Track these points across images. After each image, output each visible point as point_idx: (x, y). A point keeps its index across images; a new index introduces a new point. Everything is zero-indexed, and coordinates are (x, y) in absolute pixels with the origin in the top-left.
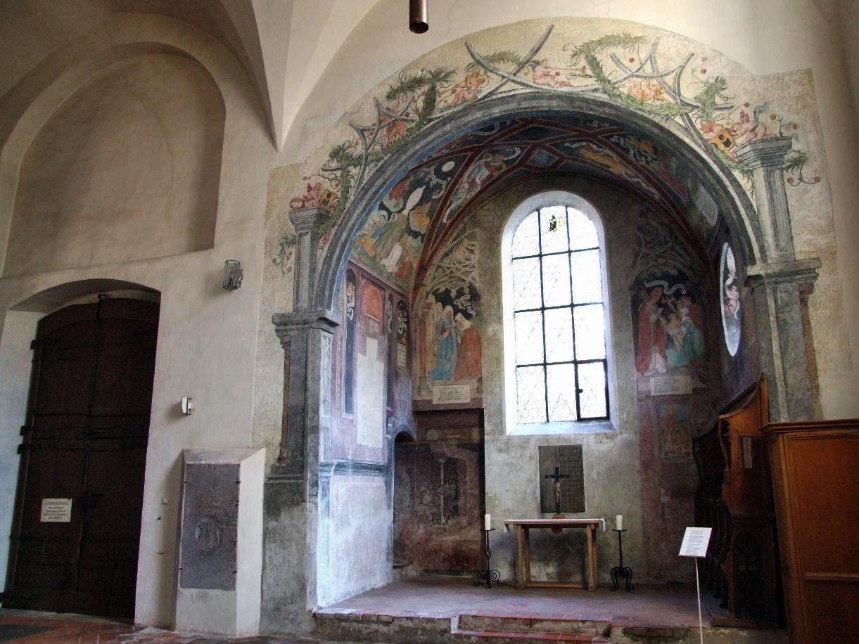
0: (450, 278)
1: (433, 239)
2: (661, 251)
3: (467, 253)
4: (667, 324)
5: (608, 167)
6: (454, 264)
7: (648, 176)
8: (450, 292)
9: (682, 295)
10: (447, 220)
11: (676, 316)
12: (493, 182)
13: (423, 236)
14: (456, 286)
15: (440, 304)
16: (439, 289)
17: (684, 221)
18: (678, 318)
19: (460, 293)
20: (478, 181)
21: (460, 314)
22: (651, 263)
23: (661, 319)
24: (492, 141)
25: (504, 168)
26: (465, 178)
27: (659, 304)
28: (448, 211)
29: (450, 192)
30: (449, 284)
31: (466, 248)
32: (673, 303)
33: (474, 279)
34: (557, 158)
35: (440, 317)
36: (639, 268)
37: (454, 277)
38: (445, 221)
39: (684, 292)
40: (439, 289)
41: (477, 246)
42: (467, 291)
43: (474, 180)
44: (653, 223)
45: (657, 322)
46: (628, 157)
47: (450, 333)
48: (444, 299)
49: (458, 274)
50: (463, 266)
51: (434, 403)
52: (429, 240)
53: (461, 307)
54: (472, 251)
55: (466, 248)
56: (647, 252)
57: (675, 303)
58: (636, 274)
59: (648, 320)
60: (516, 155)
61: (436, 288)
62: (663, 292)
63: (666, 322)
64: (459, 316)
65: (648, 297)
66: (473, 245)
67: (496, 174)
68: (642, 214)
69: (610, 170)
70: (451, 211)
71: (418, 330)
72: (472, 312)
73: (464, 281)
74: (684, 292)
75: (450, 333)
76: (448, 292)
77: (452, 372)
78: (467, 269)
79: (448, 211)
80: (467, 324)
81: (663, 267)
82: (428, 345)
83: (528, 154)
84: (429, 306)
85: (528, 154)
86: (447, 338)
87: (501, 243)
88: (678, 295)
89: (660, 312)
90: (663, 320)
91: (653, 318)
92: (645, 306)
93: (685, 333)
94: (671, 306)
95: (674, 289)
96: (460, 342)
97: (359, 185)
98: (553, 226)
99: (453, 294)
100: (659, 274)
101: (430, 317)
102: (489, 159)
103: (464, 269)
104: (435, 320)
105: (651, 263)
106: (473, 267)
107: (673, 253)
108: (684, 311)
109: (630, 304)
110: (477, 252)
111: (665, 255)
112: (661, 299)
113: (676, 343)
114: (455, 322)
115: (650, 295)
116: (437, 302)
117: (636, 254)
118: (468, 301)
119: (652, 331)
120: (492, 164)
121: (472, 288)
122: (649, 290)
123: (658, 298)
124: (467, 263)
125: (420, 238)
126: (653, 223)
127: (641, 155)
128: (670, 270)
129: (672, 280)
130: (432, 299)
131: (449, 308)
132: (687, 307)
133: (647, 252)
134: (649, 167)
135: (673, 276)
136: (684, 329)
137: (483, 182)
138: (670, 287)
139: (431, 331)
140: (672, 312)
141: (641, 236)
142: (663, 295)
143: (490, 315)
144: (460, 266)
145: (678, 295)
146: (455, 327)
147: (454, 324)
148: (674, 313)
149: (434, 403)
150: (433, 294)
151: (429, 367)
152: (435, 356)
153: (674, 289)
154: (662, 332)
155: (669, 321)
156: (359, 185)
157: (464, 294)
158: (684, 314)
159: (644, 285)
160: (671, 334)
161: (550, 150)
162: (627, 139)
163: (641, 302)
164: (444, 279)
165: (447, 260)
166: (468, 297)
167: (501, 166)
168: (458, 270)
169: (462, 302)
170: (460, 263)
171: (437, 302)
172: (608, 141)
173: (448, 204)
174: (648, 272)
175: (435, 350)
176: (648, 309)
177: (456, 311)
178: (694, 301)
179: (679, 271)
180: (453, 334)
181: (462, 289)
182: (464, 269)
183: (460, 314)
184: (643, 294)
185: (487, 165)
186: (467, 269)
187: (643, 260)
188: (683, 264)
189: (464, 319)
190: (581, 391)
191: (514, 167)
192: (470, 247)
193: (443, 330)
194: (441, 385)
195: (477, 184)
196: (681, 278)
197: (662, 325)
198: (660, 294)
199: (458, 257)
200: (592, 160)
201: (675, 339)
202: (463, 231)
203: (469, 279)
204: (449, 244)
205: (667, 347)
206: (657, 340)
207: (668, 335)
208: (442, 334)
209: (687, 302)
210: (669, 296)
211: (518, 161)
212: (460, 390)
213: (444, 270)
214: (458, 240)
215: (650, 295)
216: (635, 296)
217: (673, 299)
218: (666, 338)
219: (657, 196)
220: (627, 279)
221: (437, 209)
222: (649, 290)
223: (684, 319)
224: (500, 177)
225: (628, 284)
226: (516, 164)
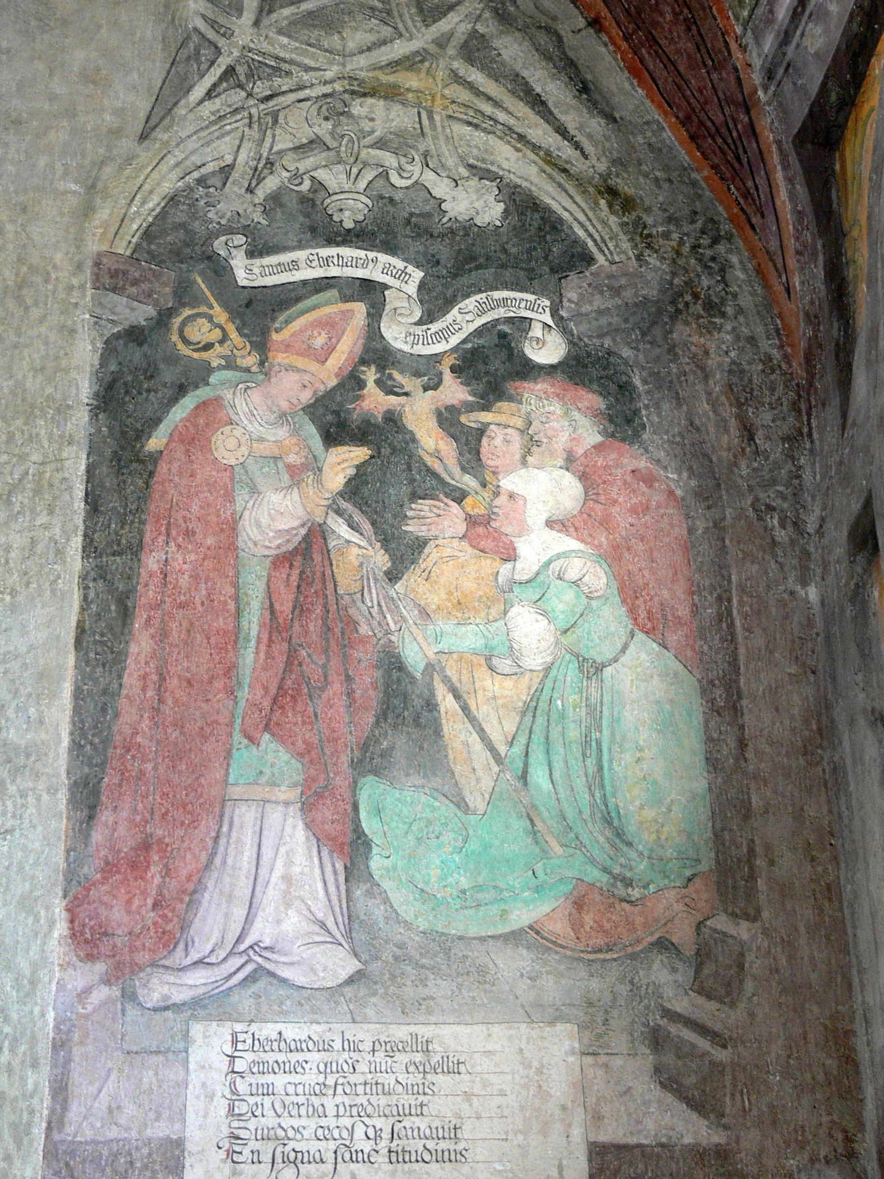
2: (386, 54)
4: (393, 576)
11: (472, 521)
23: (342, 529)
57: (470, 420)
58: (168, 187)
59: (232, 527)
62: (373, 333)
63: (381, 560)
65: (251, 360)
81: (389, 160)
93: (534, 661)
107: (476, 76)
115: (261, 346)
128: (441, 188)
132: (570, 462)
148: (460, 496)
163: (181, 390)
174: (271, 184)
187: (237, 97)
188: (549, 159)
197: (346, 581)
201: (447, 703)
215: (261, 346)
220: (87, 210)
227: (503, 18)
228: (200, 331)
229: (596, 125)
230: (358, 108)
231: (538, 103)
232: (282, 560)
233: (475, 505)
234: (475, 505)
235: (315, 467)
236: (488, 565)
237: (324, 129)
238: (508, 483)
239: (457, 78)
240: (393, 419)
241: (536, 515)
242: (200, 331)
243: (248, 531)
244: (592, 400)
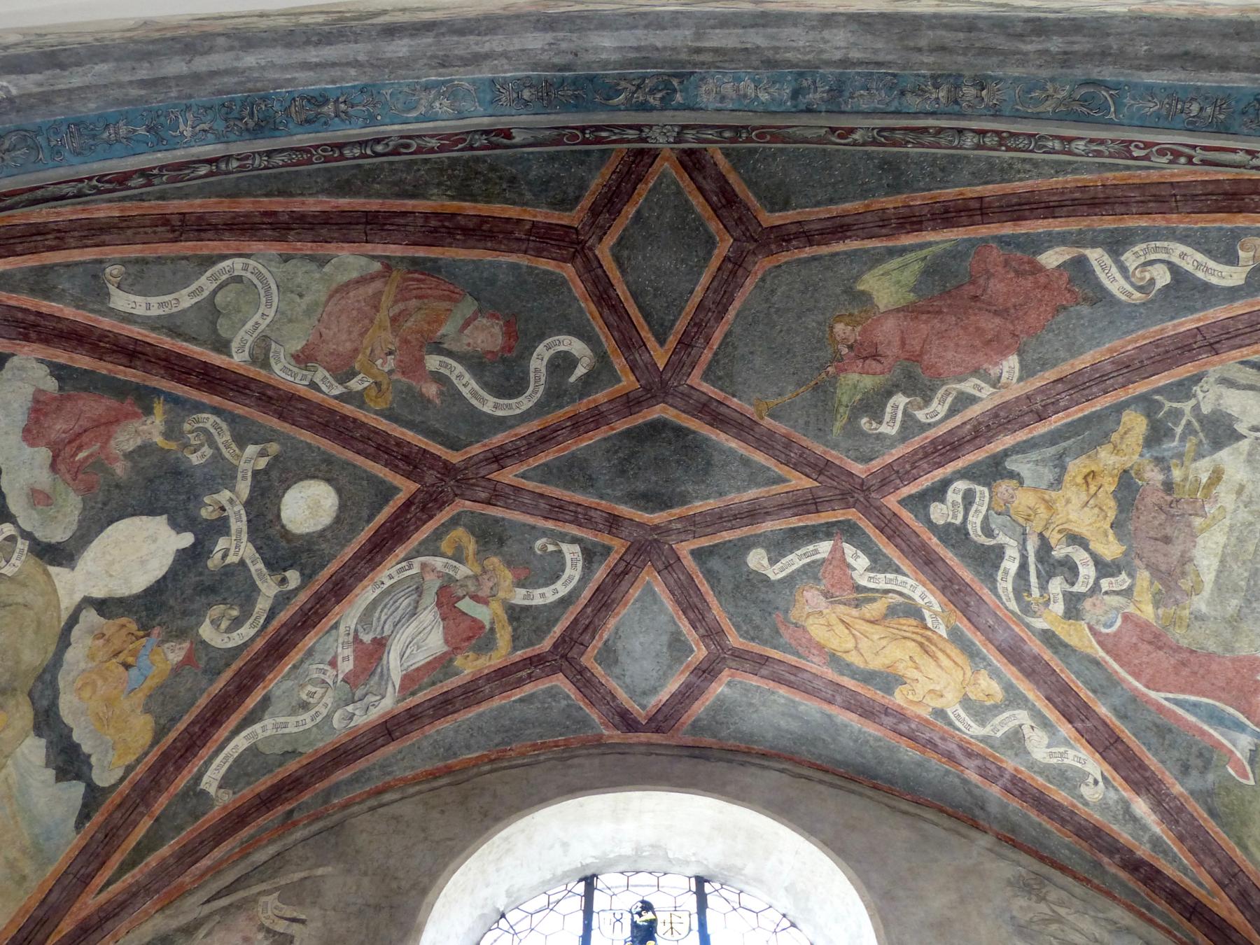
1: (132, 841)
10: (225, 783)
12: (444, 705)
13: (94, 796)
20: (395, 664)
24: (499, 458)
25: (502, 653)
28: (240, 743)
38: (211, 781)
43: (381, 644)
46: (985, 593)
66: (294, 920)
67: (469, 666)
70: (253, 751)
79: (240, 743)
87: (419, 930)
125: (76, 790)
137: (411, 681)
167: (492, 630)
195: (385, 677)
202: (278, 862)
214: (241, 894)
224: (471, 693)
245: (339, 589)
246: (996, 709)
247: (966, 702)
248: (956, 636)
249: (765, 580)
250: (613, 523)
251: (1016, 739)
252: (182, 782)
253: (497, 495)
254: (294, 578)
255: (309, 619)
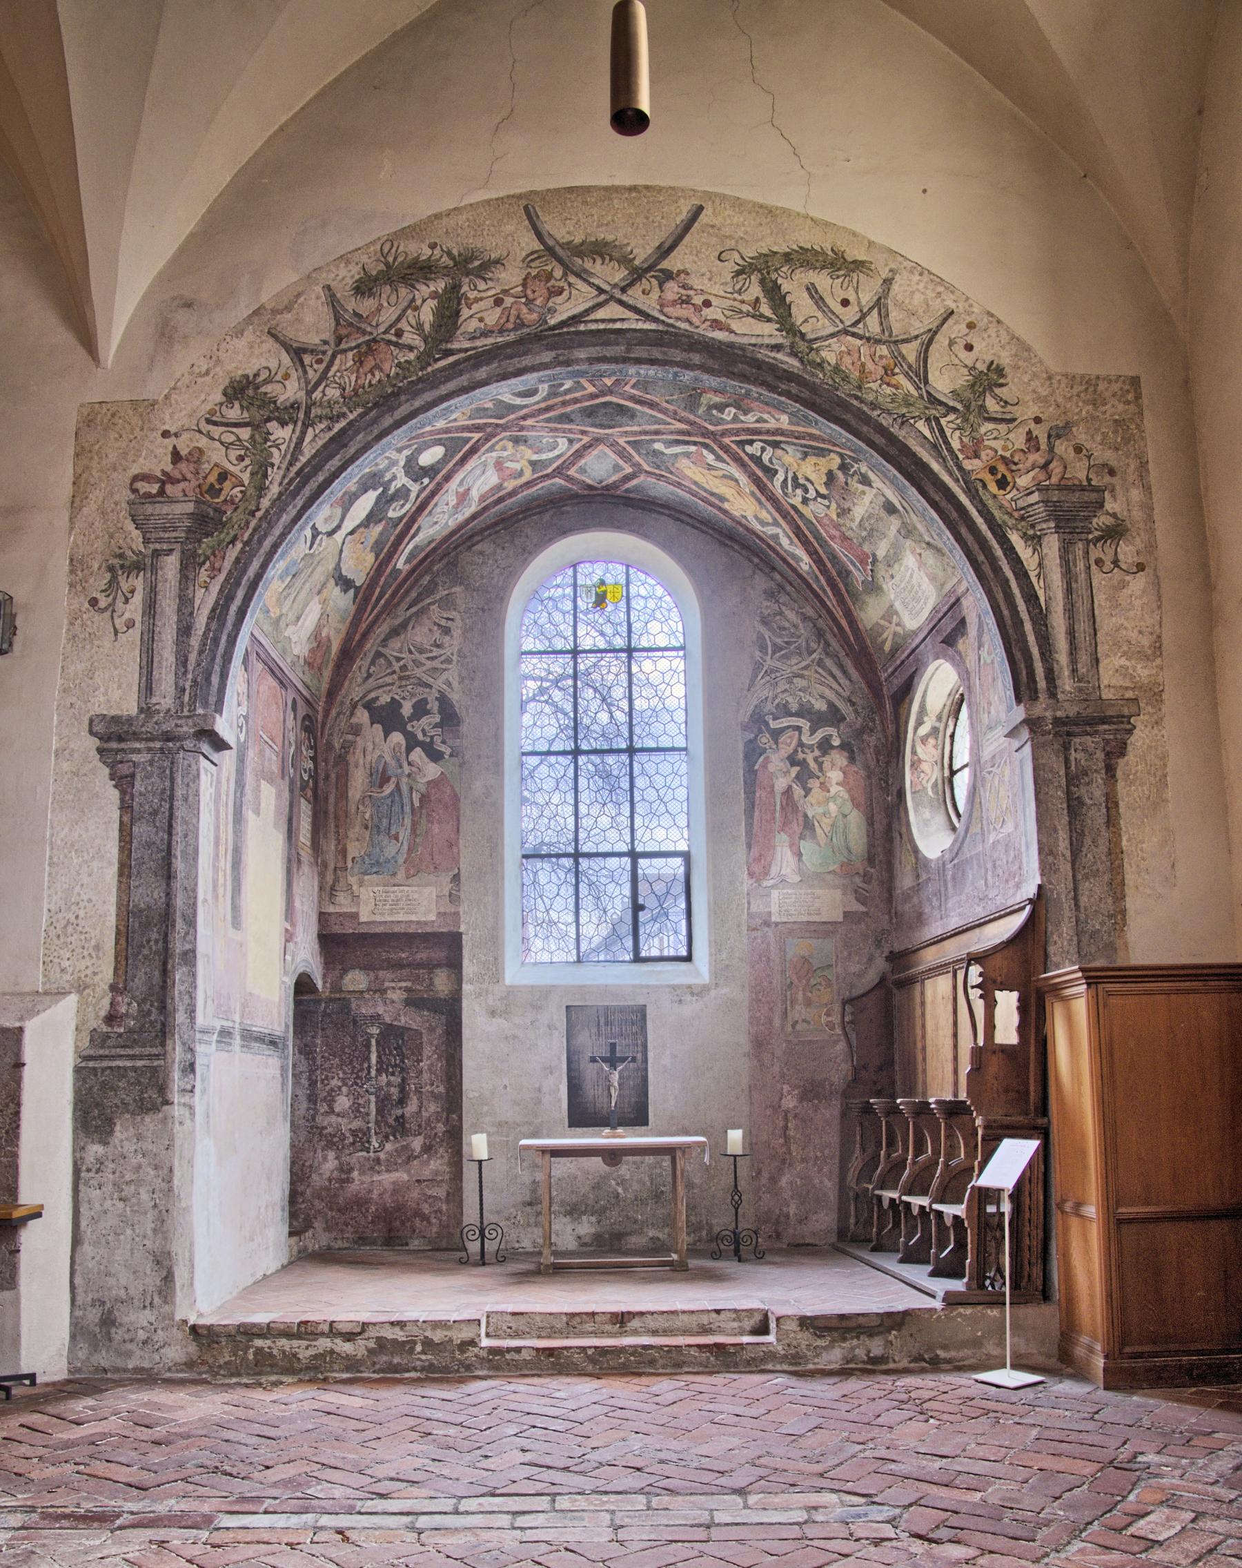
0: (401, 678)
1: (374, 598)
3: (437, 634)
5: (722, 499)
6: (410, 652)
7: (798, 527)
8: (400, 706)
9: (833, 747)
14: (412, 695)
15: (378, 727)
16: (377, 698)
17: (849, 615)
18: (824, 787)
19: (421, 709)
21: (418, 750)
22: (783, 685)
26: (453, 485)
27: (792, 760)
28: (411, 546)
29: (421, 508)
30: (399, 691)
31: (435, 623)
32: (816, 760)
33: (449, 684)
34: (629, 470)
35: (378, 753)
36: (762, 691)
37: (408, 677)
38: (400, 565)
39: (836, 742)
40: (377, 698)
41: (459, 623)
42: (434, 706)
44: (788, 613)
45: (788, 792)
47: (398, 786)
48: (388, 718)
49: (418, 672)
50: (428, 658)
51: (363, 919)
52: (366, 600)
53: (420, 737)
54: (447, 631)
55: (435, 623)
56: (778, 664)
58: (755, 703)
59: (772, 787)
60: (556, 452)
61: (373, 695)
62: (800, 739)
63: (803, 793)
64: (417, 754)
68: (770, 595)
69: (726, 506)
70: (416, 547)
71: (333, 776)
72: (442, 748)
73: (430, 687)
74: (836, 742)
75: (398, 786)
76: (395, 705)
77: (401, 861)
78: (436, 663)
79: (411, 546)
80: (432, 770)
82: (353, 808)
83: (579, 455)
84: (356, 730)
85: (579, 455)
86: (392, 794)
88: (825, 746)
89: (793, 775)
90: (798, 791)
91: (781, 784)
92: (767, 760)
94: (812, 765)
95: (819, 734)
96: (417, 804)
97: (291, 464)
98: (600, 600)
99: (407, 709)
100: (794, 707)
101: (359, 752)
102: (505, 454)
103: (429, 664)
104: (368, 758)
105: (783, 685)
106: (448, 661)
107: (820, 670)
108: (835, 776)
109: (741, 756)
110: (457, 633)
111: (806, 673)
112: (796, 751)
113: (818, 830)
114: (409, 764)
115: (776, 743)
116: (372, 724)
117: (758, 666)
118: (436, 726)
119: (778, 807)
120: (509, 464)
121: (443, 700)
122: (776, 734)
123: (790, 750)
124: (436, 652)
126: (788, 613)
127: (796, 485)
128: (813, 701)
129: (818, 720)
130: (363, 716)
131: (397, 738)
133: (778, 664)
134: (806, 511)
135: (819, 711)
136: (833, 807)
138: (813, 731)
139: (358, 782)
140: (812, 775)
141: (767, 634)
142: (801, 744)
143: (479, 757)
144: (422, 658)
145: (825, 746)
146: (409, 775)
147: (407, 769)
148: (818, 778)
149: (363, 919)
150: (365, 707)
151: (354, 850)
152: (366, 828)
153: (819, 734)
154: (795, 809)
155: (808, 791)
156: (291, 464)
157: (427, 712)
158: (834, 782)
159: (767, 724)
160: (810, 814)
161: (622, 454)
162: (779, 452)
164: (388, 680)
165: (395, 644)
166: (437, 719)
168: (418, 664)
169: (424, 726)
170: (421, 651)
171: (372, 724)
172: (739, 451)
173: (412, 531)
175: (367, 816)
176: (771, 768)
177: (412, 742)
178: (852, 759)
179: (831, 705)
180: (405, 789)
181: (425, 701)
182: (429, 664)
183: (418, 750)
184: (765, 739)
185: (499, 465)
186: (436, 663)
188: (837, 692)
189: (426, 760)
190: (642, 908)
191: (547, 475)
192: (443, 622)
193: (385, 779)
194: (377, 885)
196: (833, 716)
197: (796, 798)
198: (795, 742)
199: (418, 639)
200: (695, 483)
203: (439, 684)
204: (402, 614)
205: (802, 837)
206: (785, 824)
207: (806, 816)
208: (381, 786)
209: (840, 759)
210: (811, 747)
211: (555, 466)
212: (416, 896)
213: (390, 664)
215: (776, 743)
216: (751, 741)
217: (817, 753)
218: (801, 819)
219: (805, 563)
220: (738, 711)
221: (392, 538)
222: (776, 734)
223: (834, 789)
225: (740, 720)
226: (549, 470)
227: (827, 654)
228: (764, 740)
229: (847, 683)
230: (795, 680)
231: (834, 677)
232: (783, 794)
233: (822, 780)
234: (822, 780)
235: (788, 772)
236: (825, 793)
237: (787, 686)
238: (829, 774)
239: (816, 672)
240: (804, 760)
241: (834, 782)
242: (764, 740)
243: (776, 787)
244: (846, 754)
245: (448, 478)
246: (768, 524)
247: (756, 517)
248: (753, 494)
249: (663, 453)
250: (583, 433)
251: (775, 537)
252: (390, 567)
253: (522, 429)
254: (426, 481)
255: (433, 494)
